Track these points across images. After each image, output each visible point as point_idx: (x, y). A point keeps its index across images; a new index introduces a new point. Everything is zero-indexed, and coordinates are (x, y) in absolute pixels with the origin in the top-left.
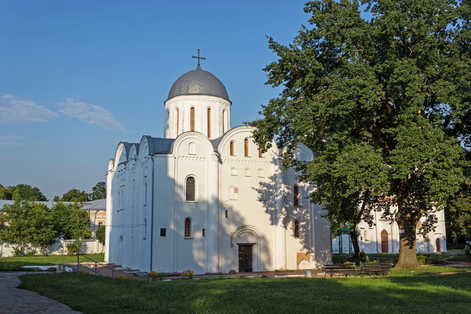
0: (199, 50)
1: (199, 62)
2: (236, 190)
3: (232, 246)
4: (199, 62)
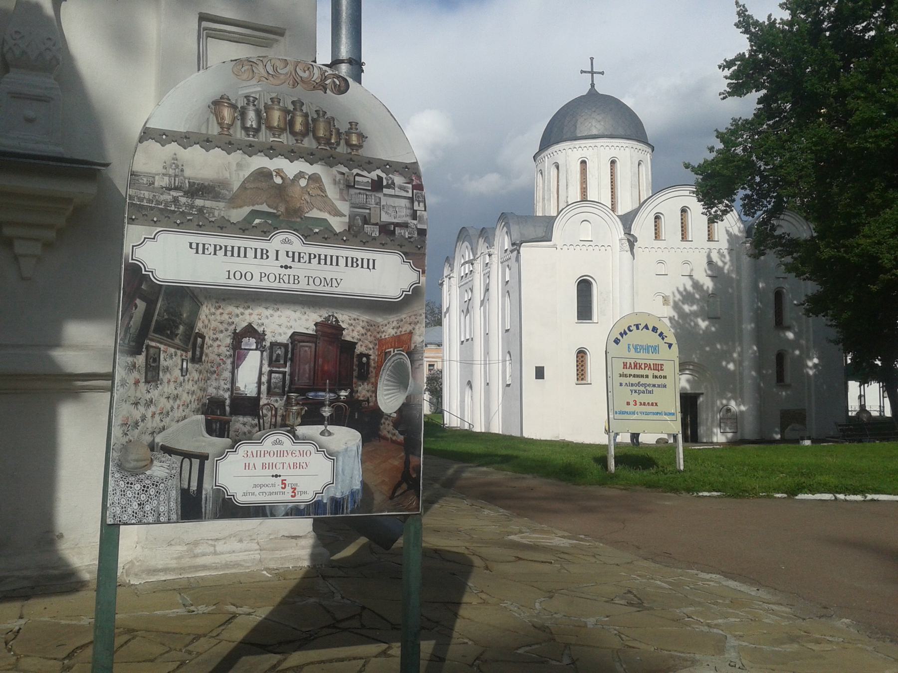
0: (592, 59)
1: (593, 81)
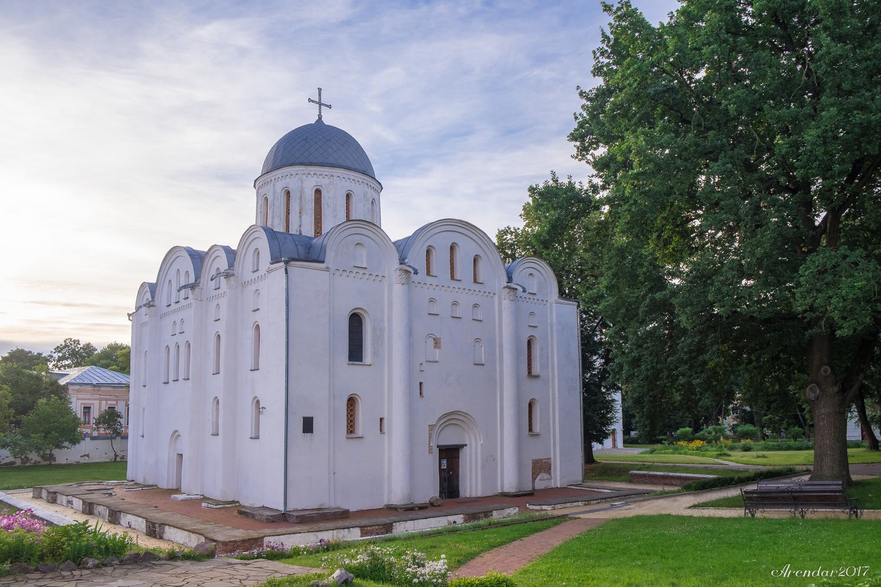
0: (320, 90)
1: (320, 112)
2: (437, 343)
3: (430, 450)
4: (320, 112)
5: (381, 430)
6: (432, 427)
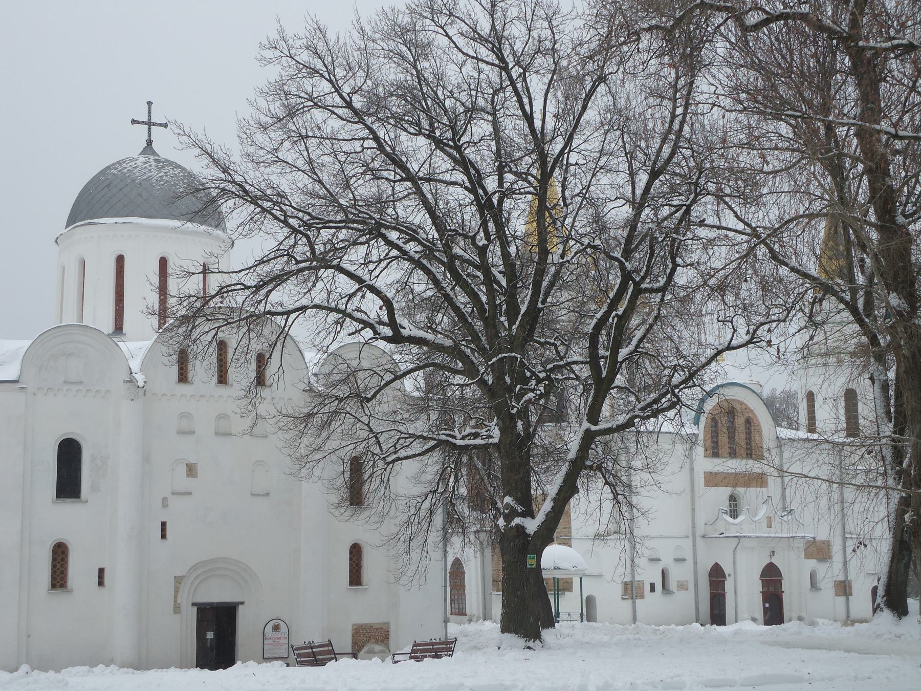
0: (150, 104)
1: (149, 135)
2: (191, 470)
3: (177, 609)
4: (149, 135)
5: (101, 583)
6: (179, 580)
